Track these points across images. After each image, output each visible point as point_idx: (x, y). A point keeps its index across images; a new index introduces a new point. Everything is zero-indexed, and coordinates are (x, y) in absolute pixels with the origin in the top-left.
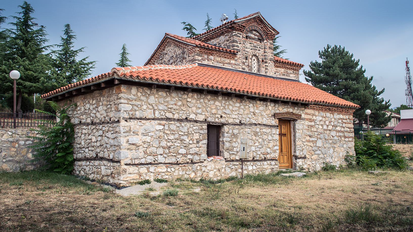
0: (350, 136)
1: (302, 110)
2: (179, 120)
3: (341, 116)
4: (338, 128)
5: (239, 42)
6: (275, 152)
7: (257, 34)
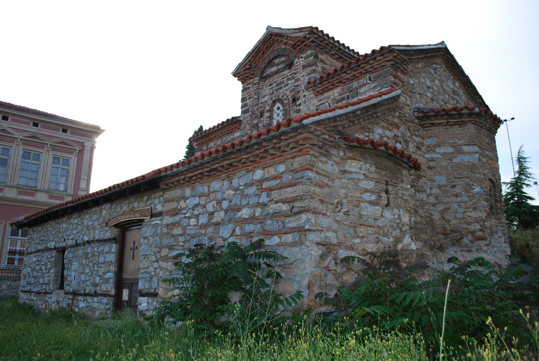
0: (291, 225)
1: (159, 198)
2: (43, 251)
3: (258, 174)
4: (245, 213)
5: (248, 97)
6: (107, 281)
7: (283, 59)
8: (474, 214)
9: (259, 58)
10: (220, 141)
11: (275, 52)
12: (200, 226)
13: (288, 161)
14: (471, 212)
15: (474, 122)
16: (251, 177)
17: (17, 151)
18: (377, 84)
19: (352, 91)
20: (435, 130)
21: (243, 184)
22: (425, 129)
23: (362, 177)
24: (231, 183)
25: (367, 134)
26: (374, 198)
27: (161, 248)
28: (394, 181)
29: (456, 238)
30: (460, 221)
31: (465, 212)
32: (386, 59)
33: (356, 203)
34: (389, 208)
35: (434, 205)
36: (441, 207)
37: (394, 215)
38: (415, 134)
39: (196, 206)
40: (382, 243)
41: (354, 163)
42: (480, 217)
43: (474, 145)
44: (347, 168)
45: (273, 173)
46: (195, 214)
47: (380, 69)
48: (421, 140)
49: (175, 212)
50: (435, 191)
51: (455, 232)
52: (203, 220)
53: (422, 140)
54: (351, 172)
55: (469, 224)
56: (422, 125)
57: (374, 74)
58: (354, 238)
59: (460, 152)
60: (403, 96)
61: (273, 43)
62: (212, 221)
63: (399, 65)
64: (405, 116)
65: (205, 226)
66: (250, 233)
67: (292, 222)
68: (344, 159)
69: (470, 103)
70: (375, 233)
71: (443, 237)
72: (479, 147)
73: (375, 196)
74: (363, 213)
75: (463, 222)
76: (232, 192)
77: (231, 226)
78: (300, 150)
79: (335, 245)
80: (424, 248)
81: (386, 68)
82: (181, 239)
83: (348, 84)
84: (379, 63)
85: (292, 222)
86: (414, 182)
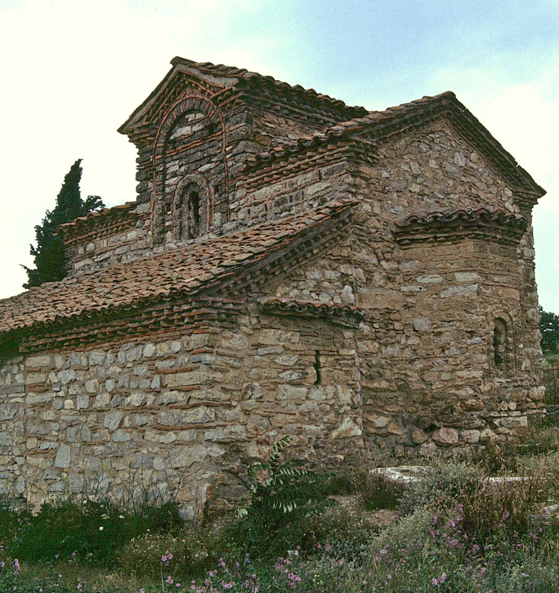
0: (188, 420)
1: (18, 364)
3: (149, 349)
4: (135, 399)
7: (199, 116)
9: (163, 108)
10: (105, 241)
11: (188, 102)
12: (79, 411)
13: (184, 338)
15: (474, 236)
16: (141, 353)
18: (329, 185)
19: (296, 189)
20: (417, 250)
21: (131, 360)
22: (403, 247)
23: (280, 350)
24: (117, 356)
25: (294, 284)
26: (295, 376)
27: (26, 435)
28: (329, 349)
30: (446, 383)
31: (454, 371)
32: (340, 149)
33: (273, 387)
34: (320, 387)
35: (411, 361)
37: (327, 395)
38: (384, 259)
39: (72, 382)
45: (166, 352)
46: (71, 393)
47: (333, 162)
48: (395, 266)
49: (44, 388)
52: (83, 403)
53: (397, 266)
54: (267, 346)
56: (399, 242)
57: (326, 168)
59: (451, 282)
60: (366, 202)
61: (183, 88)
62: (94, 406)
63: (362, 156)
64: (370, 233)
65: (84, 412)
66: (142, 426)
67: (190, 417)
69: (499, 181)
70: (297, 421)
72: (480, 273)
73: (297, 374)
75: (450, 385)
76: (119, 370)
77: (118, 415)
78: (197, 328)
79: (244, 441)
80: (391, 425)
81: (341, 161)
82: (54, 426)
83: (292, 177)
84: (330, 153)
85: (190, 417)
86: (379, 332)
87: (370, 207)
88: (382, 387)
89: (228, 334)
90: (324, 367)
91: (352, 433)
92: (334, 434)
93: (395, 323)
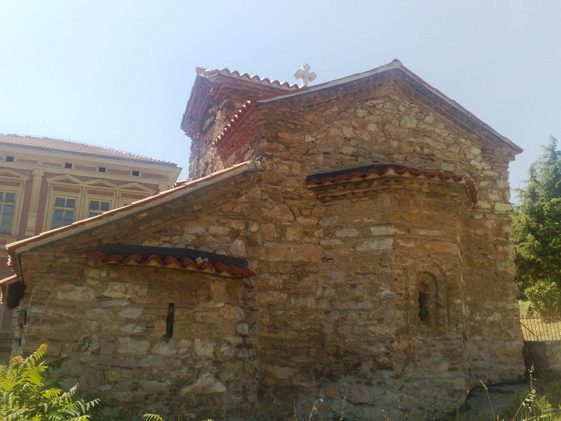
8: (378, 330)
14: (375, 325)
17: (83, 201)
20: (338, 206)
25: (167, 239)
26: (138, 330)
29: (352, 363)
33: (111, 338)
36: (336, 316)
37: (178, 349)
40: (143, 389)
41: (118, 286)
42: (386, 334)
43: (388, 224)
44: (106, 294)
50: (330, 292)
51: (351, 354)
55: (370, 344)
58: (100, 383)
59: (368, 236)
68: (105, 282)
71: (335, 360)
74: (119, 351)
80: (299, 377)
87: (288, 168)
88: (288, 337)
89: (68, 286)
90: (177, 320)
91: (212, 390)
92: (185, 390)
93: (310, 274)
